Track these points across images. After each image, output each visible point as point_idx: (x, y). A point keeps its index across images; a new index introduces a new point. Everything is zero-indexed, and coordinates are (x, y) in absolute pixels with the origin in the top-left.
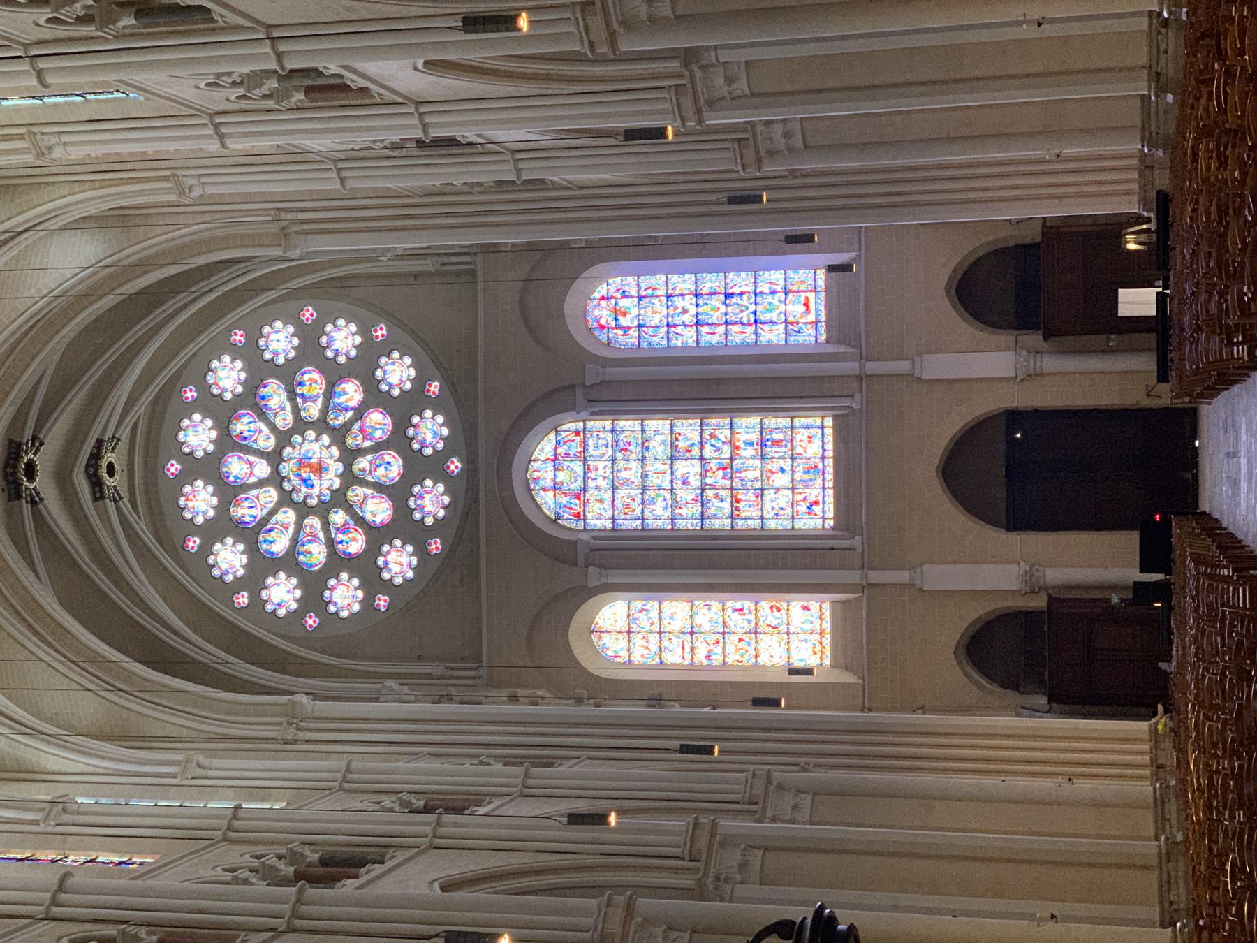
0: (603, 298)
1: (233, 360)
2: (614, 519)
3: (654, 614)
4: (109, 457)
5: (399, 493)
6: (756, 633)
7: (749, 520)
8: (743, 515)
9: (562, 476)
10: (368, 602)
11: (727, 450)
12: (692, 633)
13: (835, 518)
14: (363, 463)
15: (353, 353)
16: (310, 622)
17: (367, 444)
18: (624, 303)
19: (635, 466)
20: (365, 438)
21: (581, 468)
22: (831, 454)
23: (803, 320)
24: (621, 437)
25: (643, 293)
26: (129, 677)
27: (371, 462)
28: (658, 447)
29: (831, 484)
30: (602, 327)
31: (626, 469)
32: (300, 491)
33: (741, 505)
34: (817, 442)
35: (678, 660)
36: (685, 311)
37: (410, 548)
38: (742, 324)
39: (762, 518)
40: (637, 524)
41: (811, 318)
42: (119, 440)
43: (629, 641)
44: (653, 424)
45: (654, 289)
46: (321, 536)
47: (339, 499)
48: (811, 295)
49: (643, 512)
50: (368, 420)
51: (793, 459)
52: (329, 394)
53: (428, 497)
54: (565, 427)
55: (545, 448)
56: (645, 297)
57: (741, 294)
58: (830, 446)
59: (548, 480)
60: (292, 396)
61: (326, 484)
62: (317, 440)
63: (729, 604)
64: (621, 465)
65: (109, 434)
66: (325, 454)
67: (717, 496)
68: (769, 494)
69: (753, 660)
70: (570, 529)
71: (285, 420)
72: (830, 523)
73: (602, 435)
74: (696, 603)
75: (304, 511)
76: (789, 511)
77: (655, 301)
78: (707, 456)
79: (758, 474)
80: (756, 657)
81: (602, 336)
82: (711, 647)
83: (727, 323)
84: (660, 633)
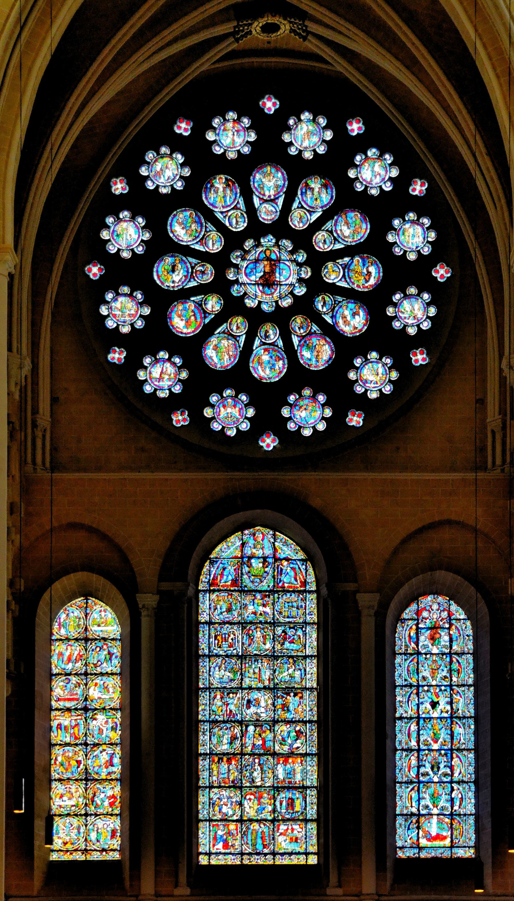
0: (450, 614)
2: (210, 623)
3: (107, 668)
4: (285, 27)
5: (238, 377)
6: (86, 780)
7: (207, 772)
8: (214, 767)
10: (114, 337)
12: (86, 709)
13: (210, 866)
15: (397, 325)
16: (95, 270)
17: (295, 340)
20: (302, 337)
21: (265, 588)
23: (421, 833)
25: (455, 658)
26: (32, 48)
28: (287, 673)
29: (246, 862)
30: (418, 613)
31: (264, 637)
32: (243, 259)
33: (224, 766)
36: (434, 705)
37: (177, 389)
38: (419, 767)
39: (211, 787)
40: (203, 648)
41: (423, 842)
42: (305, 39)
43: (77, 640)
44: (312, 668)
45: (459, 672)
46: (193, 284)
48: (447, 842)
50: (322, 342)
51: (273, 821)
52: (350, 294)
53: (235, 412)
54: (311, 571)
55: (288, 549)
57: (452, 768)
58: (286, 861)
59: (254, 551)
60: (350, 251)
61: (251, 290)
62: (300, 280)
63: (118, 749)
65: (313, 27)
66: (284, 289)
67: (234, 738)
69: (57, 776)
70: (200, 574)
71: (321, 241)
72: (203, 860)
73: (301, 612)
74: (119, 715)
75: (220, 262)
76: (219, 817)
78: (276, 728)
80: (60, 780)
81: (409, 613)
83: (419, 750)
84: (86, 674)
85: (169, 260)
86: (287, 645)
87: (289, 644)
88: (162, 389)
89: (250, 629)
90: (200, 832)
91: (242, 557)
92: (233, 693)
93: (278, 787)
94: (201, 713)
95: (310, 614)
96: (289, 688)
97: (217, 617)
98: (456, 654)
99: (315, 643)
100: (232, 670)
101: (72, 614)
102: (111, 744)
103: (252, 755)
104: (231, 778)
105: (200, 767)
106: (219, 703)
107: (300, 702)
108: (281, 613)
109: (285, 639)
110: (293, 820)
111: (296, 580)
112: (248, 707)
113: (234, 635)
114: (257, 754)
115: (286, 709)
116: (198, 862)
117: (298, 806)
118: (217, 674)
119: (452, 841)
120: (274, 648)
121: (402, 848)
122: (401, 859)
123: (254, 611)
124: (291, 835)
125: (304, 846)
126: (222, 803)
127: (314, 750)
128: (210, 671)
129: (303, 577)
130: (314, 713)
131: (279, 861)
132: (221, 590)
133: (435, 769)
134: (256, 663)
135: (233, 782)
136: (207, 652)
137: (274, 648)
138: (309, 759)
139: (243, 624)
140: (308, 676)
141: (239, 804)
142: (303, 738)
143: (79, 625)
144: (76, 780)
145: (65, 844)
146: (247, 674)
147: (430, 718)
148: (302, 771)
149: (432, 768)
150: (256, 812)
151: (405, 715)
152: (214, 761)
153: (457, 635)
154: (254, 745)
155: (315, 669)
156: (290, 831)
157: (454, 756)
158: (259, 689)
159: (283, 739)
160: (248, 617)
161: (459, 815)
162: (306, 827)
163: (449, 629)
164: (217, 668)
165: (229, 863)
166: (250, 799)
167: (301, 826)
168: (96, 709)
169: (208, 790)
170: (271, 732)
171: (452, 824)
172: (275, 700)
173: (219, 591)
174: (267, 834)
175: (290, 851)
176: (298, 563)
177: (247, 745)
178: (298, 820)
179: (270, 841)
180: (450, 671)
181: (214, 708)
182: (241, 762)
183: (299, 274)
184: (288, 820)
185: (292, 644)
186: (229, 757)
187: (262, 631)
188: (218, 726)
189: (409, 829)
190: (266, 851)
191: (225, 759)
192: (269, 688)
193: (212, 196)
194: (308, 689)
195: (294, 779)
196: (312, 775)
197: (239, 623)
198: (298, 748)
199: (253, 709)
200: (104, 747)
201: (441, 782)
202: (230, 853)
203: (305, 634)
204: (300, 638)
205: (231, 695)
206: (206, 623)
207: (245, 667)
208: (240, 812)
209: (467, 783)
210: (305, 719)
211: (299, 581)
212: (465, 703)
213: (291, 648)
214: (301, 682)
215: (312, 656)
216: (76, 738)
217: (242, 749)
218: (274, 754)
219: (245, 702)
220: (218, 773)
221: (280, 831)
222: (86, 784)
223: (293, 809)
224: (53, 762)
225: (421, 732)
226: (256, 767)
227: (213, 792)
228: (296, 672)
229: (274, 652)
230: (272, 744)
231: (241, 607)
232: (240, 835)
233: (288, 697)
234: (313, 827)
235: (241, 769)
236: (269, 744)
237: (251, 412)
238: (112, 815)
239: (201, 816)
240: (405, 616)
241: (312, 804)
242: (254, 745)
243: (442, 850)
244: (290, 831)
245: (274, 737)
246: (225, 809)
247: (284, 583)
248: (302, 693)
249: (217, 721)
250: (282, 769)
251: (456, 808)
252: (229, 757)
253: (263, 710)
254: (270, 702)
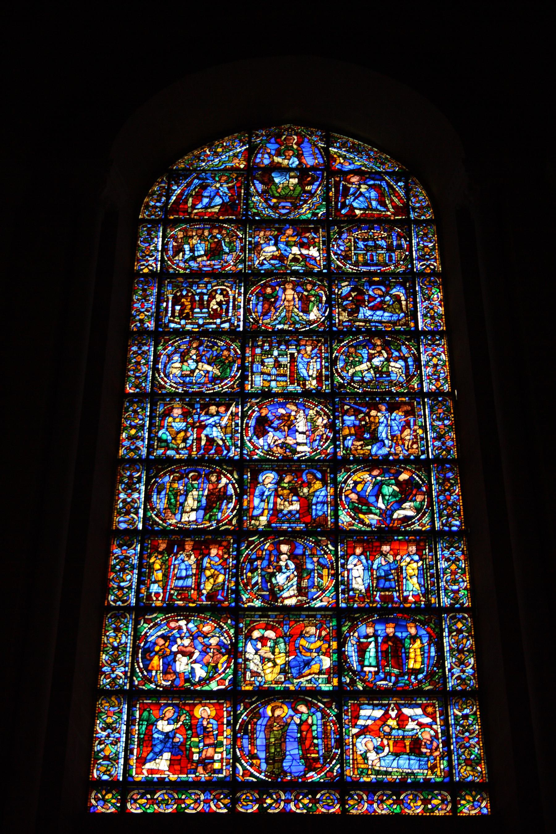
2: (163, 276)
22: (359, 807)
34: (406, 764)
39: (143, 610)
67: (216, 499)
72: (105, 805)
86: (365, 312)
87: (369, 313)
89: (265, 286)
92: (218, 405)
93: (350, 609)
94: (126, 443)
96: (377, 394)
97: (182, 265)
104: (208, 587)
106: (179, 425)
107: (408, 423)
108: (346, 258)
109: (359, 303)
111: (382, 203)
112: (261, 432)
113: (226, 295)
114: (284, 533)
115: (367, 436)
118: (176, 368)
120: (330, 317)
123: (276, 253)
125: (444, 764)
126: (174, 649)
128: (156, 360)
129: (400, 199)
130: (449, 443)
132: (194, 220)
134: (283, 347)
135: (211, 596)
136: (151, 325)
137: (330, 317)
141: (228, 652)
142: (419, 498)
146: (257, 367)
150: (283, 671)
152: (155, 549)
154: (276, 512)
155: (443, 357)
156: (392, 723)
158: (289, 397)
160: (262, 264)
162: (445, 715)
164: (176, 357)
166: (263, 640)
167: (430, 710)
170: (325, 484)
172: (336, 418)
174: (316, 730)
176: (387, 178)
177: (256, 512)
179: (328, 749)
181: (163, 434)
182: (238, 550)
185: (379, 313)
186: (201, 540)
187: (299, 289)
188: (172, 472)
190: (314, 777)
194: (429, 394)
195: (401, 591)
196: (455, 582)
199: (272, 437)
202: (197, 785)
203: (411, 294)
204: (400, 301)
205: (213, 409)
207: (253, 355)
208: (230, 671)
210: (423, 457)
211: (390, 206)
213: (375, 318)
214: (408, 382)
215: (432, 333)
217: (240, 522)
218: (337, 534)
219: (252, 423)
220: (166, 576)
221: (361, 722)
226: (282, 563)
227: (147, 621)
228: (392, 364)
229: (332, 325)
231: (243, 250)
232: (228, 732)
233: (373, 413)
235: (236, 566)
236: (318, 510)
239: (104, 681)
241: (461, 651)
242: (276, 512)
244: (392, 723)
245: (337, 495)
246: (182, 665)
247: (352, 209)
248: (410, 404)
249: (170, 461)
250: (360, 567)
252: (201, 540)
253: (301, 438)
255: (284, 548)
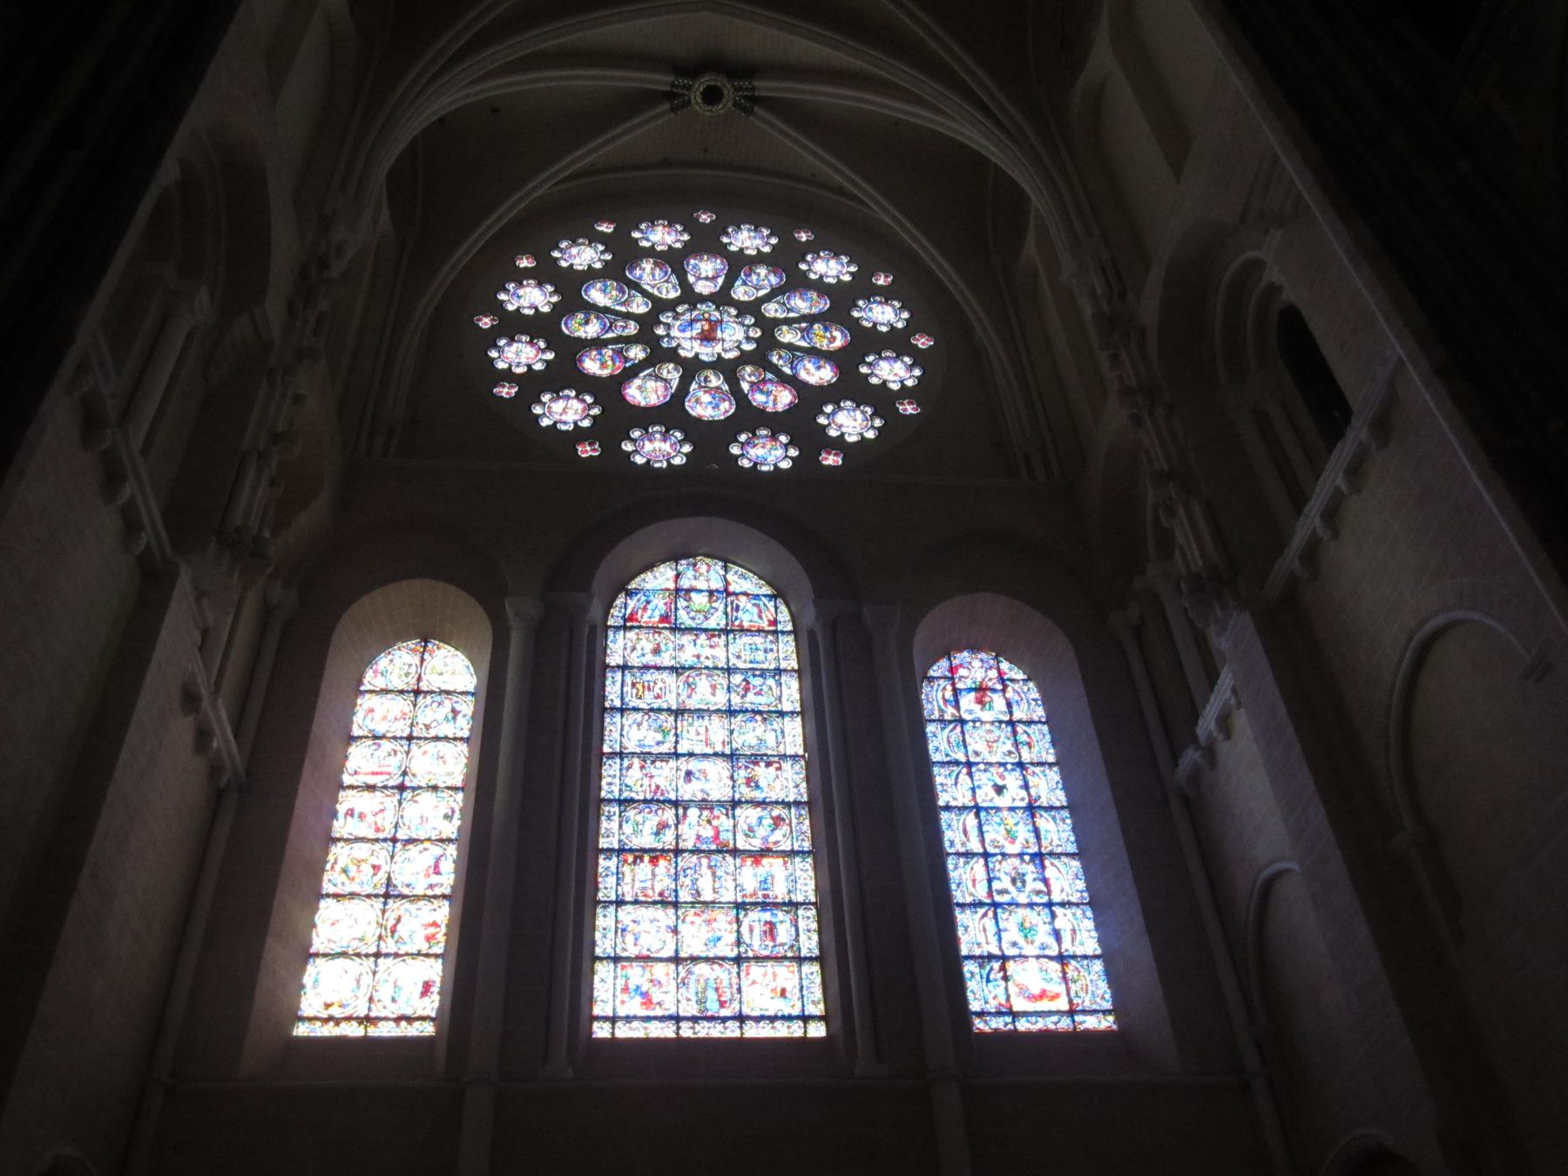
0: (1000, 673)
1: (851, 274)
2: (624, 668)
3: (447, 730)
6: (387, 896)
8: (626, 869)
9: (700, 600)
11: (756, 844)
13: (613, 1041)
14: (716, 381)
17: (745, 386)
18: (998, 702)
19: (720, 700)
20: (752, 384)
24: (771, 682)
27: (718, 388)
28: (750, 735)
29: (686, 1031)
30: (952, 670)
31: (714, 687)
33: (645, 867)
35: (351, 765)
36: (999, 790)
39: (620, 903)
41: (1019, 1005)
43: (402, 692)
46: (610, 335)
47: (660, 354)
49: (636, 709)
51: (738, 960)
52: (814, 353)
53: (666, 447)
56: (1015, 733)
57: (1046, 881)
64: (721, 680)
67: (662, 826)
68: (666, 917)
69: (332, 890)
71: (772, 310)
72: (601, 1031)
73: (770, 656)
74: (460, 796)
75: (647, 323)
76: (633, 951)
77: (1009, 746)
78: (738, 811)
79: (707, 896)
80: (336, 896)
82: (370, 819)
83: (986, 855)
84: (410, 738)
85: (581, 316)
86: (750, 697)
88: (565, 423)
90: (597, 979)
91: (677, 590)
95: (785, 659)
98: (1020, 721)
99: (797, 696)
100: (660, 729)
101: (397, 661)
102: (441, 840)
103: (696, 851)
104: (658, 889)
105: (600, 870)
109: (747, 689)
110: (777, 959)
116: (591, 1033)
117: (784, 933)
119: (1071, 1002)
121: (981, 1014)
122: (982, 1034)
124: (773, 985)
125: (799, 1004)
127: (807, 846)
131: (752, 1031)
133: (1019, 884)
135: (661, 894)
136: (618, 703)
138: (798, 859)
139: (677, 670)
140: (788, 739)
143: (407, 674)
144: (368, 896)
145: (327, 1006)
147: (998, 809)
148: (787, 878)
149: (1014, 881)
151: (953, 803)
152: (625, 861)
153: (1017, 698)
154: (699, 837)
157: (1047, 863)
159: (751, 829)
161: (1074, 957)
162: (800, 971)
163: (1004, 691)
165: (652, 1035)
168: (419, 788)
169: (612, 909)
171: (1064, 973)
173: (640, 627)
174: (726, 983)
175: (771, 1013)
178: (785, 958)
180: (1016, 744)
181: (628, 781)
183: (746, 332)
184: (767, 958)
186: (655, 855)
189: (988, 981)
190: (725, 1012)
191: (646, 858)
192: (723, 755)
193: (638, 272)
197: (672, 669)
198: (776, 843)
200: (427, 844)
201: (1031, 905)
202: (656, 1018)
205: (658, 764)
206: (618, 666)
209: (1077, 905)
212: (1048, 787)
215: (792, 713)
216: (378, 830)
218: (735, 852)
219: (682, 774)
222: (385, 904)
223: (773, 939)
224: (328, 866)
225: (985, 828)
230: (730, 835)
234: (813, 971)
236: (724, 836)
237: (687, 448)
238: (427, 955)
240: (931, 673)
242: (699, 837)
243: (1055, 1018)
244: (770, 977)
249: (631, 801)
251: (1066, 944)
252: (655, 855)
254: (728, 774)
255: (704, 861)
